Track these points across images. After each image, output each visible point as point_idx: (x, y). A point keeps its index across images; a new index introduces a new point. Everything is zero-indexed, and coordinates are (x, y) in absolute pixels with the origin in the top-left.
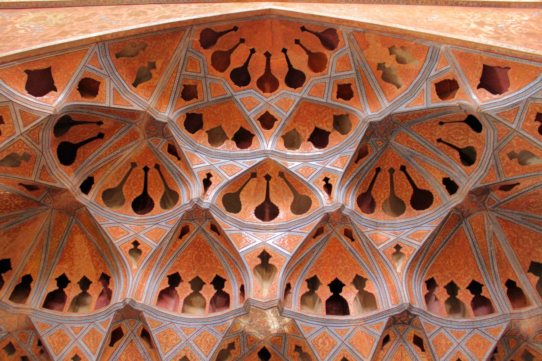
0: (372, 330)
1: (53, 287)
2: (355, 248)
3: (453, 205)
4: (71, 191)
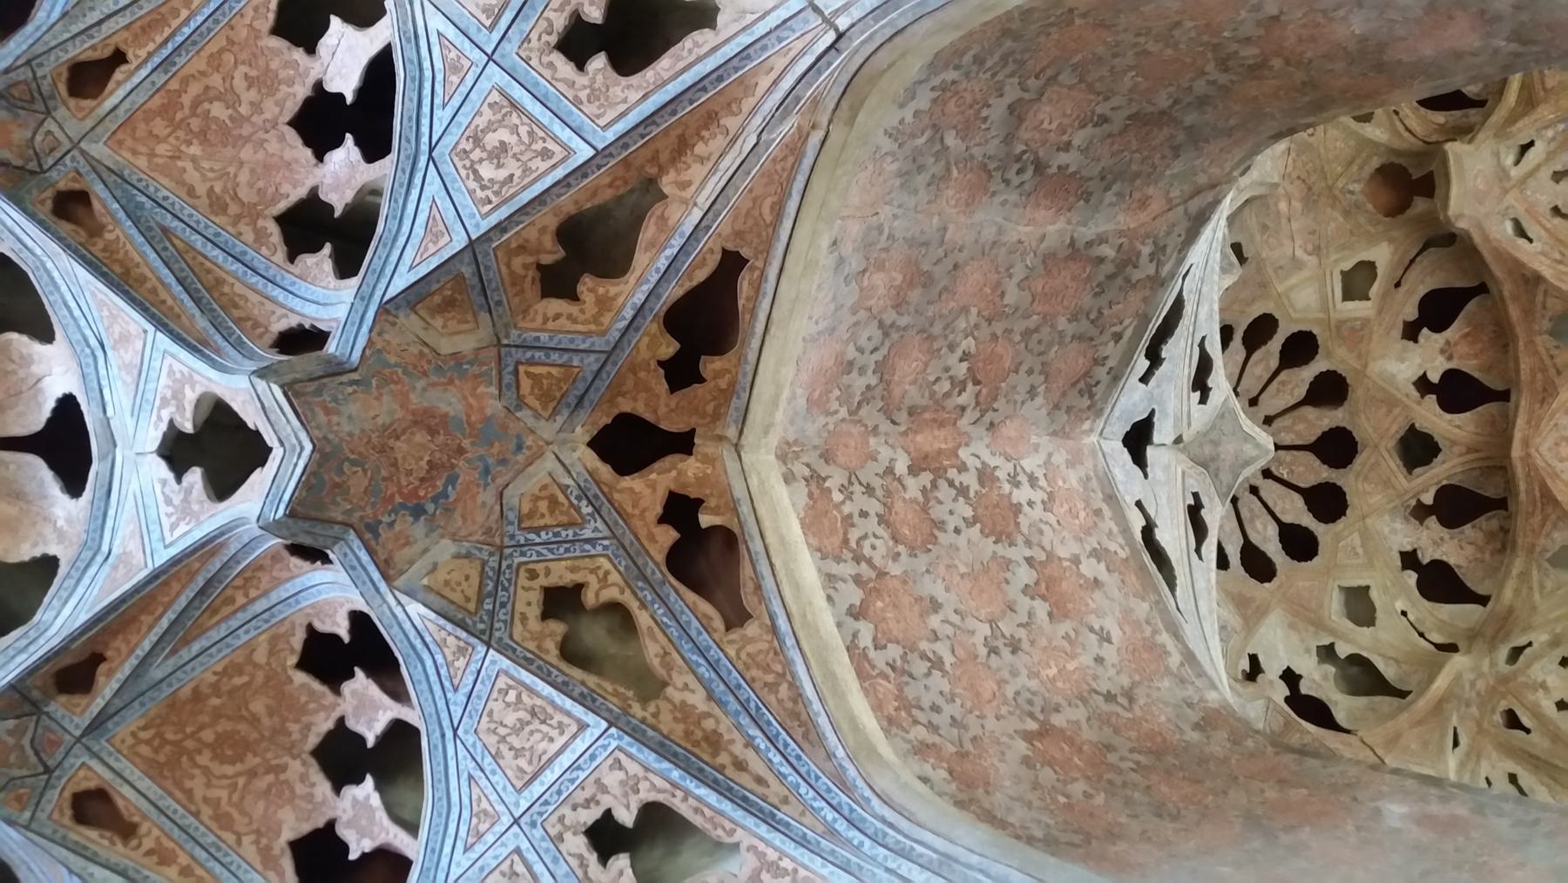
2: (151, 47)
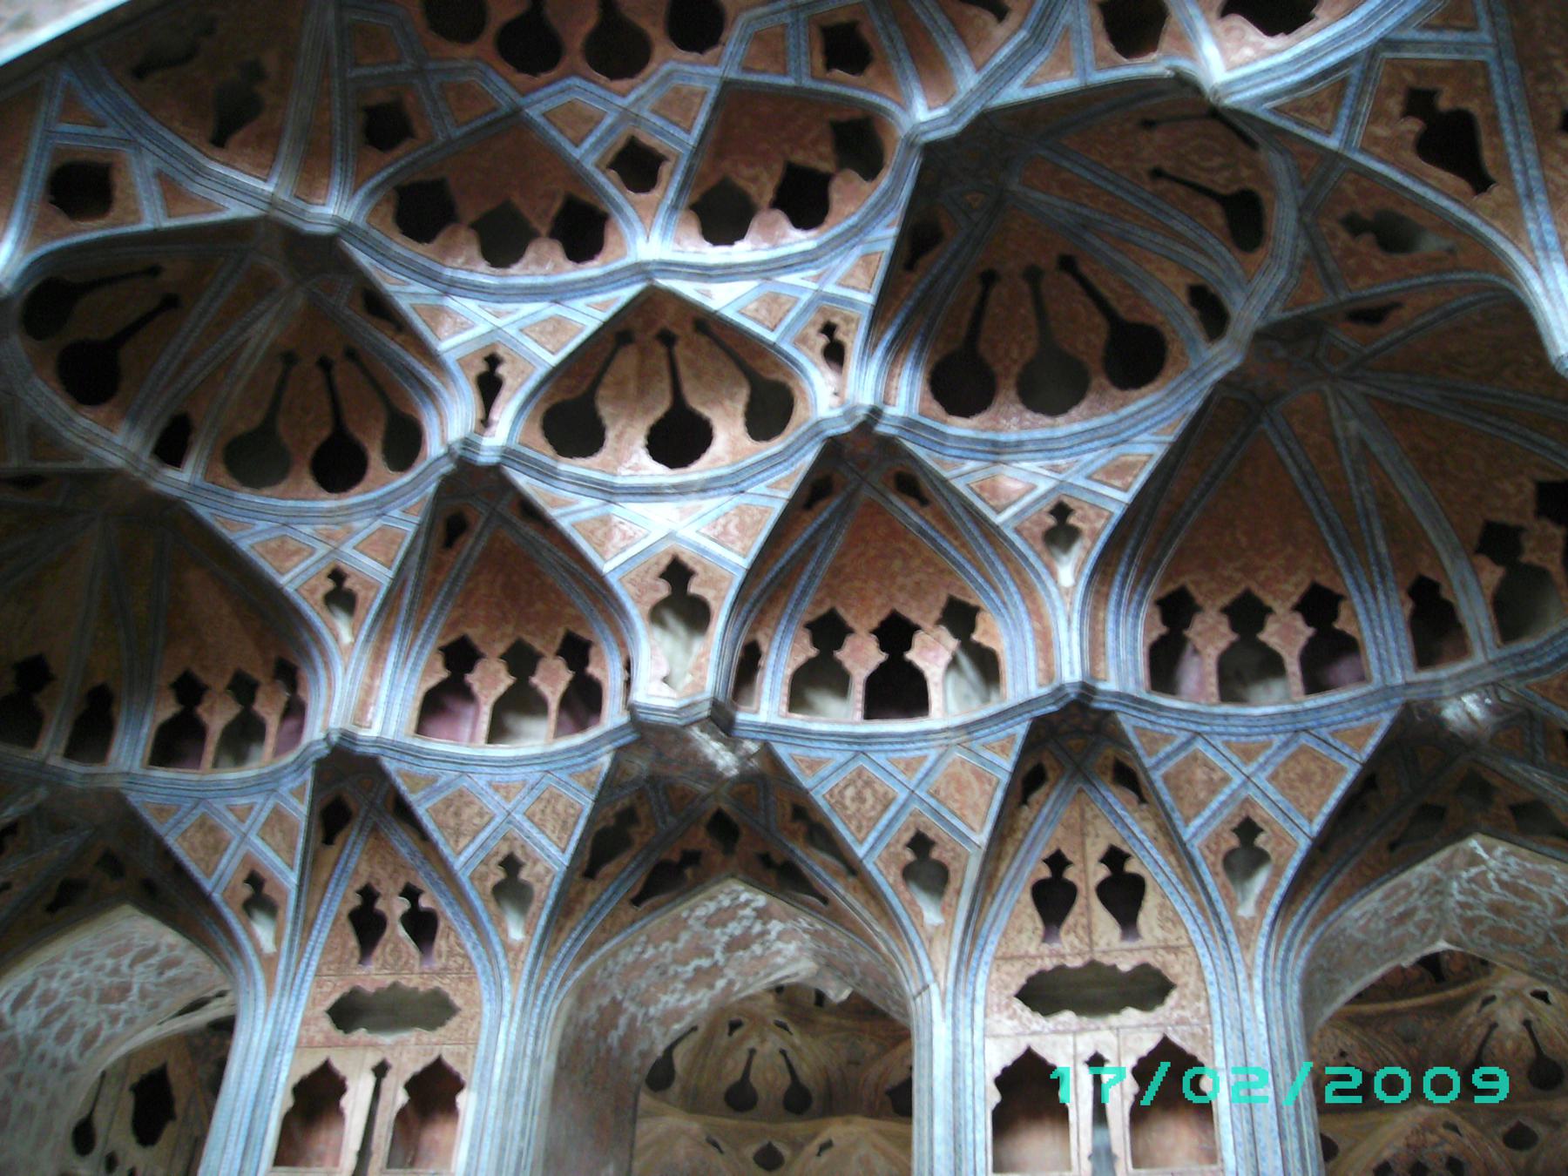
0: (988, 755)
1: (168, 709)
3: (1217, 375)
4: (130, 469)
